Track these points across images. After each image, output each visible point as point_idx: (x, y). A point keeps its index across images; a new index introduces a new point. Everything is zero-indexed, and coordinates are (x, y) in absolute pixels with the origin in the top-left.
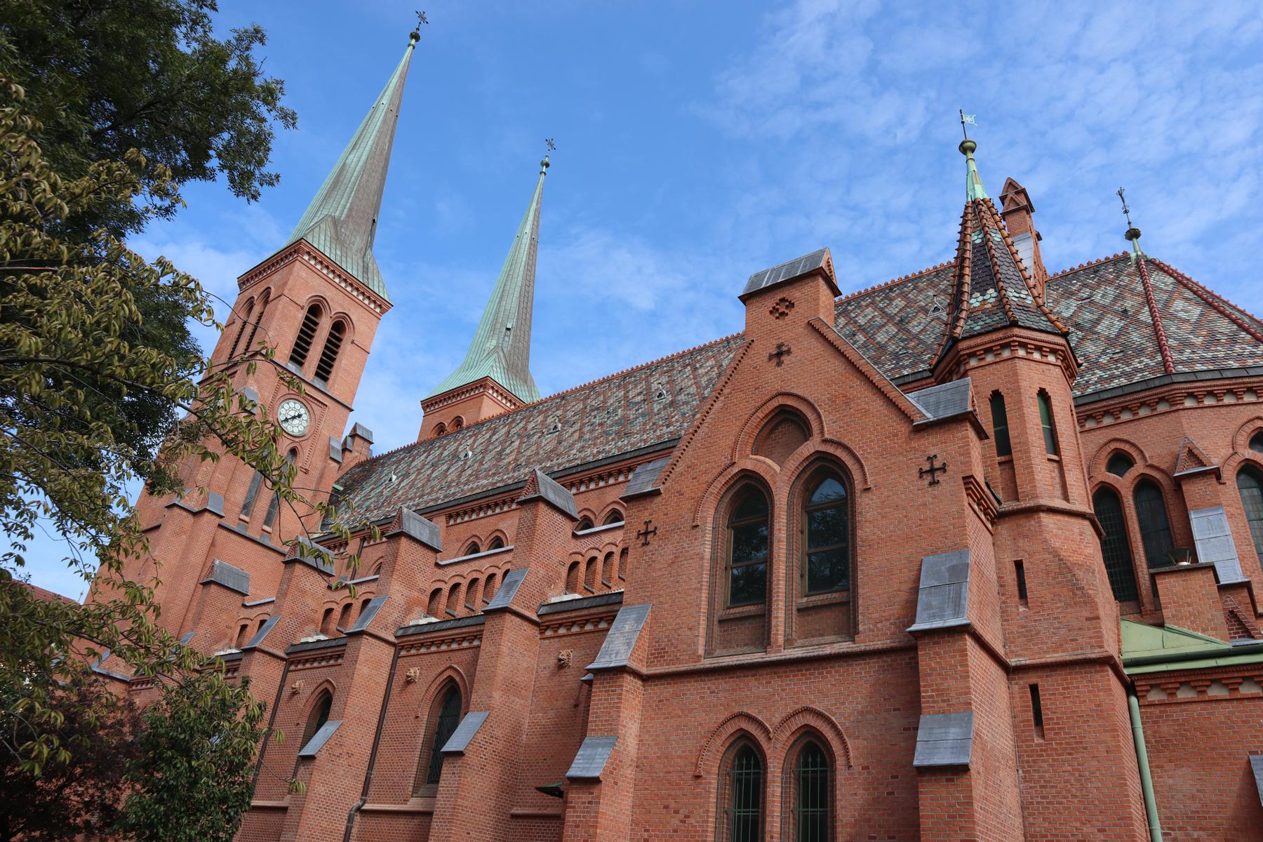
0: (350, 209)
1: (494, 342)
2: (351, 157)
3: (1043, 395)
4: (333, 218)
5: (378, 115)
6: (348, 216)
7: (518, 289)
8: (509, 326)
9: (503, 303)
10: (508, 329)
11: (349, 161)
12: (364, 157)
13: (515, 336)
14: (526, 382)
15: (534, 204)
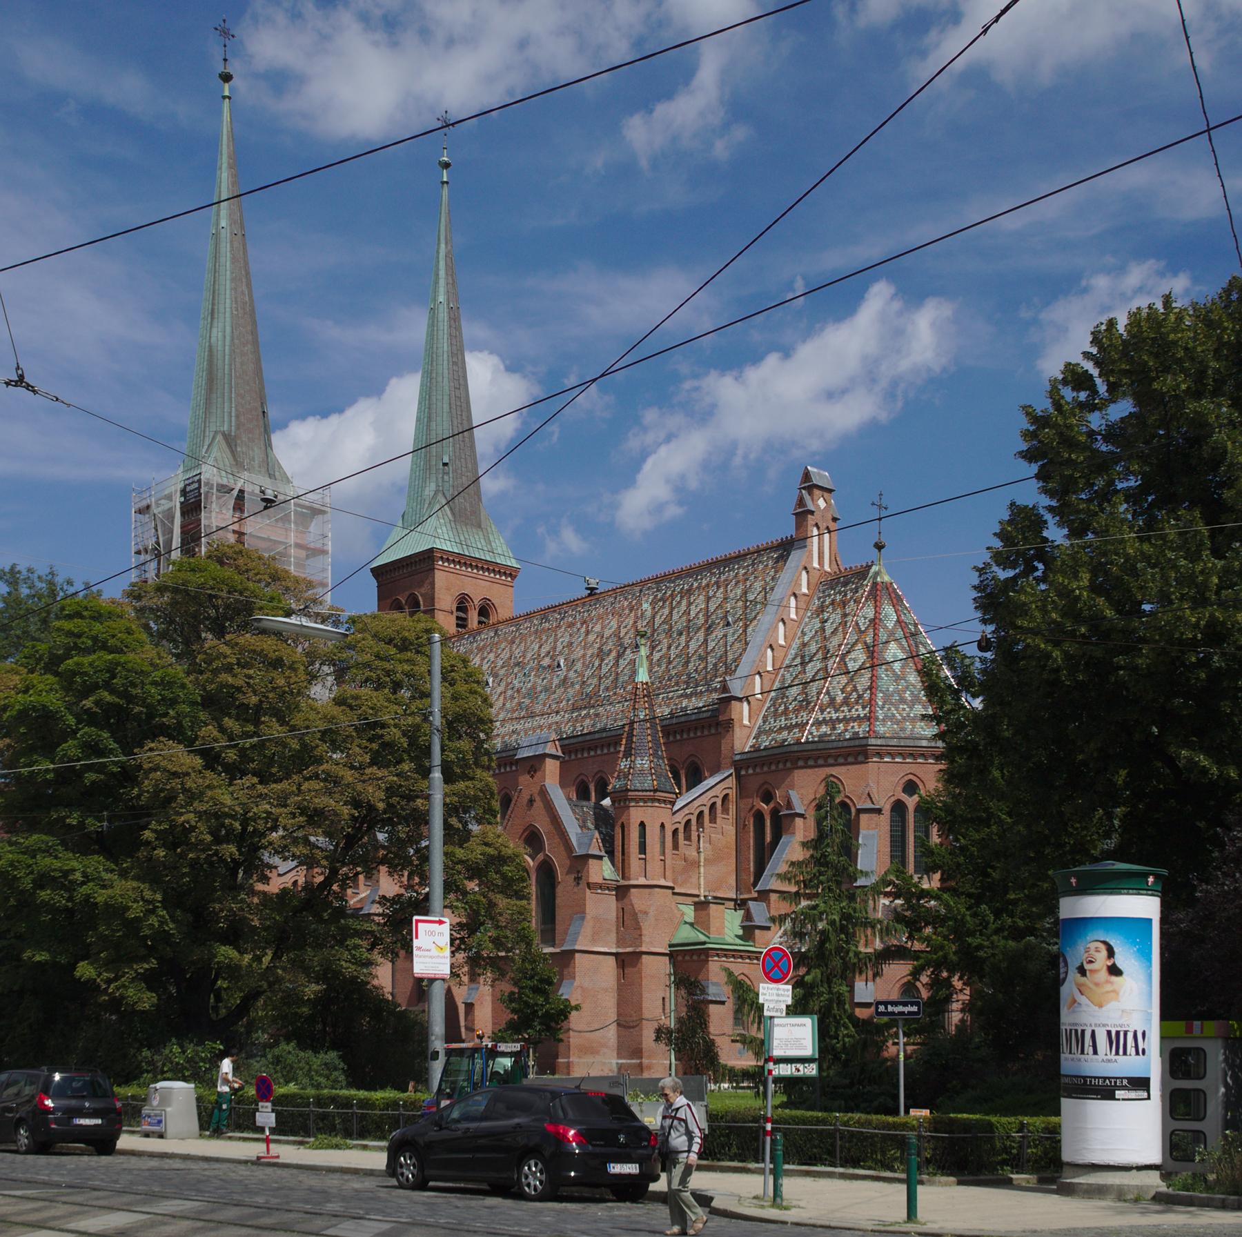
0: (237, 417)
1: (433, 486)
2: (214, 330)
3: (642, 825)
4: (224, 434)
5: (223, 245)
6: (238, 428)
7: (446, 398)
8: (446, 460)
9: (433, 425)
10: (445, 464)
11: (213, 339)
12: (228, 329)
13: (455, 471)
14: (480, 526)
15: (443, 246)
